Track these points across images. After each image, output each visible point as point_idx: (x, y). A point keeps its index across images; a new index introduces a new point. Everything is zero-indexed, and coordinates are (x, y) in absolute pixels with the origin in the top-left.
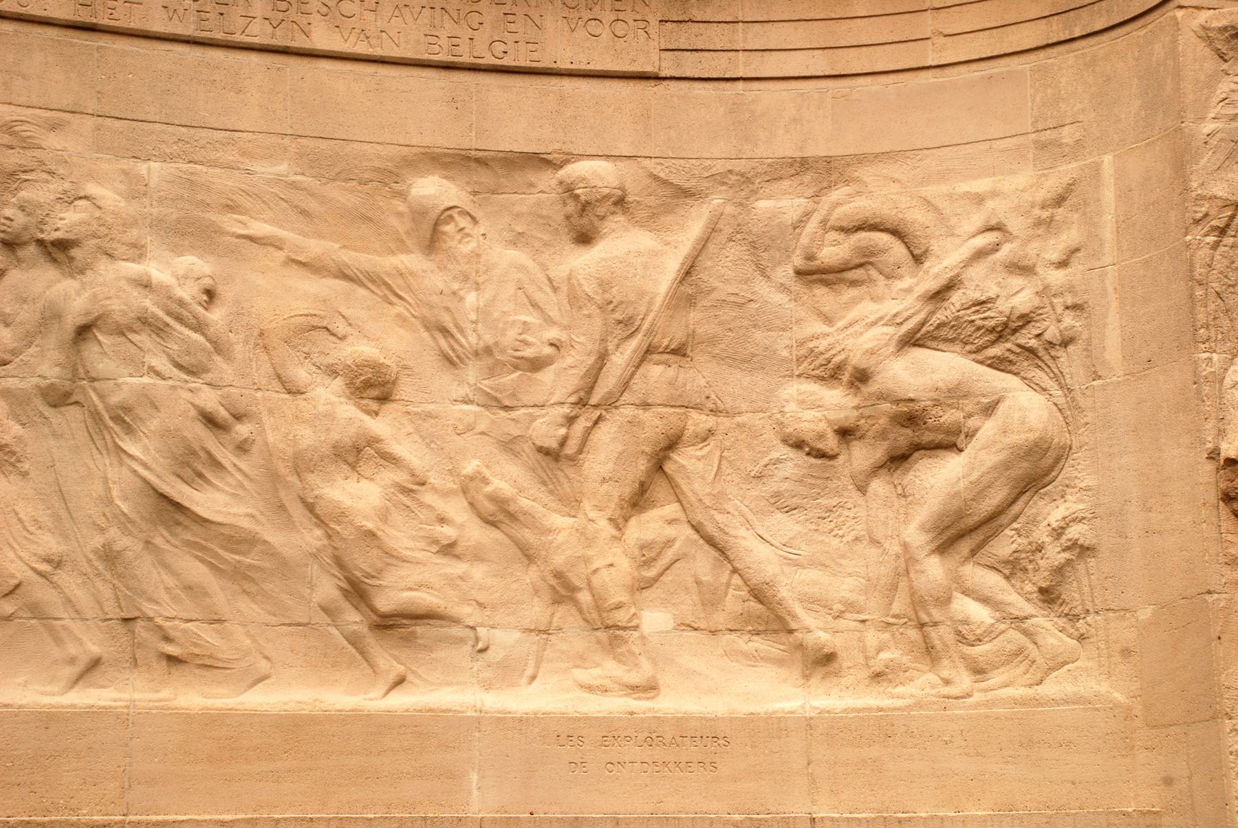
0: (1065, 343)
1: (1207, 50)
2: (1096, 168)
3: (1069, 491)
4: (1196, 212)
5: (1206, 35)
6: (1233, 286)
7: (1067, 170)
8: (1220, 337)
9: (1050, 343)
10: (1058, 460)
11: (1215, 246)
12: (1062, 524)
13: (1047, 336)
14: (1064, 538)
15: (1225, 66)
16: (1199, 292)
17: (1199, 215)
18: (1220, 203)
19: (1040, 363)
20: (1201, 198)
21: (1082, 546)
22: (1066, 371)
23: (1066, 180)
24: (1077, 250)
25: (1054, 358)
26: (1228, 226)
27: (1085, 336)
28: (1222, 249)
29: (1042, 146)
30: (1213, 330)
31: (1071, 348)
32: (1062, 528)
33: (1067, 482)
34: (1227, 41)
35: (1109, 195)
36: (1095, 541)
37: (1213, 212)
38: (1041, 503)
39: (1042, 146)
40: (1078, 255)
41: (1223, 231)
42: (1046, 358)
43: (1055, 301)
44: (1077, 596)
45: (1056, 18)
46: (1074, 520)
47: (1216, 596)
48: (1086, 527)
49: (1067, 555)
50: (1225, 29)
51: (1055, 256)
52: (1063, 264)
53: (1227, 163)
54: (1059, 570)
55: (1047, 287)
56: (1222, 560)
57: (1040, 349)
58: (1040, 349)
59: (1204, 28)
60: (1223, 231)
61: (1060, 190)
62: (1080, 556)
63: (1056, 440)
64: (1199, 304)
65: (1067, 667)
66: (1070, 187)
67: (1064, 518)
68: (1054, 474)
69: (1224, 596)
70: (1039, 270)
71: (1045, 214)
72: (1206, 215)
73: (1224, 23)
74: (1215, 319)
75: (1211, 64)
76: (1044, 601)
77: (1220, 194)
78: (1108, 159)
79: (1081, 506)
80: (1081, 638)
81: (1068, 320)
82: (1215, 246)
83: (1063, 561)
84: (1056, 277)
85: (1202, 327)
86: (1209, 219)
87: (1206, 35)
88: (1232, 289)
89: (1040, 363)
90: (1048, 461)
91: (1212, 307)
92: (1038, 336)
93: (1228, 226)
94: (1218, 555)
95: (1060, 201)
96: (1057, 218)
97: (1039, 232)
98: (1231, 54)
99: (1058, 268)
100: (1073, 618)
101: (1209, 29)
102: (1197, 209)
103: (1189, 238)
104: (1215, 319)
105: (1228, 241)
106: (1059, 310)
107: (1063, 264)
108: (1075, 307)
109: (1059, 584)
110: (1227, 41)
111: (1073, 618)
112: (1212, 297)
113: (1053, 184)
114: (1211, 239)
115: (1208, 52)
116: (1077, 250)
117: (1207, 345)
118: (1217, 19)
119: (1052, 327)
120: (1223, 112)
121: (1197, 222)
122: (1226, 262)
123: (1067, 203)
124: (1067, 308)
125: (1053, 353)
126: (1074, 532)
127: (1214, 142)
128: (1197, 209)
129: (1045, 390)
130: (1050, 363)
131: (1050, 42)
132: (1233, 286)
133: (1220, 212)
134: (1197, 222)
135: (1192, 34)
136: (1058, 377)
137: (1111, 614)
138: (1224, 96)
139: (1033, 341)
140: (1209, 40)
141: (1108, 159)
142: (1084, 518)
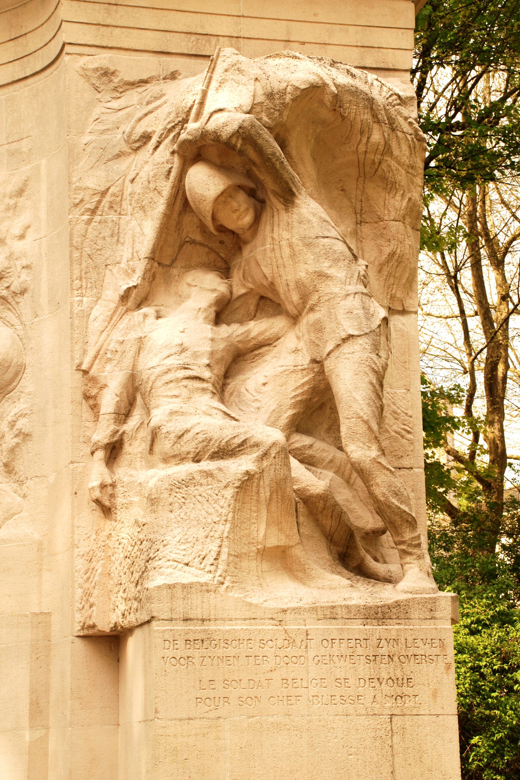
0: (23, 292)
1: (86, 84)
2: (38, 168)
3: (23, 395)
4: (75, 198)
5: (84, 74)
6: (100, 250)
7: (26, 169)
8: (89, 285)
9: (14, 292)
10: (16, 374)
11: (89, 222)
12: (14, 419)
13: (12, 288)
14: (16, 428)
15: (99, 96)
16: (76, 254)
17: (77, 201)
18: (91, 192)
19: (10, 307)
20: (80, 189)
21: (24, 433)
22: (23, 312)
23: (24, 178)
24: (29, 227)
25: (17, 303)
26: (97, 208)
27: (32, 288)
28: (93, 224)
29: (12, 154)
30: (84, 281)
31: (26, 295)
32: (15, 421)
33: (22, 389)
34: (99, 78)
35: (44, 187)
36: (31, 430)
37: (87, 198)
38: (7, 404)
39: (12, 154)
40: (30, 230)
41: (93, 212)
42: (13, 303)
43: (17, 263)
44: (21, 467)
45: (17, 62)
46: (21, 416)
47: (76, 465)
48: (27, 420)
49: (16, 440)
50: (97, 69)
51: (17, 231)
52: (22, 237)
53: (97, 164)
54: (12, 451)
55: (11, 254)
56: (82, 439)
57: (10, 297)
58: (10, 297)
59: (83, 69)
60: (93, 212)
61: (20, 185)
62: (24, 440)
63: (15, 361)
64: (75, 263)
65: (15, 517)
66: (26, 183)
67: (15, 414)
68: (15, 384)
69: (81, 464)
70: (8, 241)
71: (12, 202)
72: (82, 201)
73: (96, 65)
74: (86, 273)
75: (89, 94)
76: (7, 472)
77: (91, 186)
78: (44, 161)
79: (25, 406)
80: (24, 496)
81: (24, 276)
82: (89, 222)
83: (14, 444)
84: (18, 246)
85: (77, 279)
86: (84, 203)
87: (84, 74)
88: (99, 252)
89: (10, 307)
90: (9, 375)
91: (84, 265)
92: (8, 287)
93: (97, 208)
94: (79, 437)
95: (20, 192)
96: (19, 204)
97: (9, 215)
98: (102, 87)
99: (20, 239)
100: (21, 483)
101: (86, 70)
102: (76, 196)
103: (71, 216)
104: (86, 273)
105: (97, 218)
106: (19, 268)
107: (22, 237)
108: (26, 267)
109: (13, 460)
110: (99, 78)
111: (21, 483)
112: (85, 258)
113: (16, 182)
114: (86, 217)
115: (87, 86)
116: (29, 227)
117: (79, 291)
118: (92, 62)
119: (16, 281)
120: (96, 128)
121: (76, 205)
122: (96, 233)
123: (25, 194)
124: (23, 268)
125: (17, 299)
126: (21, 424)
127: (89, 149)
128: (76, 196)
129: (13, 326)
130: (15, 306)
131: (15, 79)
132: (100, 250)
133: (91, 198)
134: (76, 205)
135: (75, 73)
136: (19, 317)
137: (37, 480)
138: (97, 117)
139: (5, 291)
140: (87, 77)
141: (44, 161)
142: (26, 414)
